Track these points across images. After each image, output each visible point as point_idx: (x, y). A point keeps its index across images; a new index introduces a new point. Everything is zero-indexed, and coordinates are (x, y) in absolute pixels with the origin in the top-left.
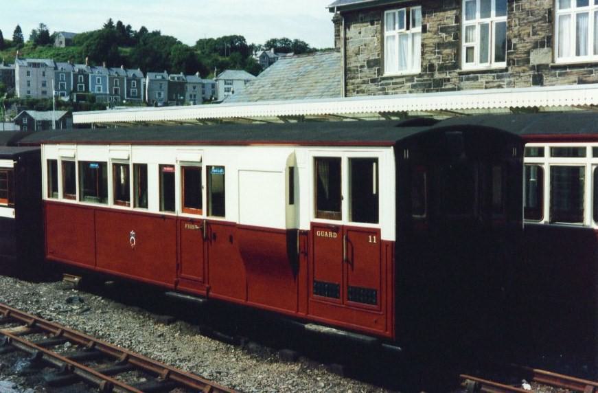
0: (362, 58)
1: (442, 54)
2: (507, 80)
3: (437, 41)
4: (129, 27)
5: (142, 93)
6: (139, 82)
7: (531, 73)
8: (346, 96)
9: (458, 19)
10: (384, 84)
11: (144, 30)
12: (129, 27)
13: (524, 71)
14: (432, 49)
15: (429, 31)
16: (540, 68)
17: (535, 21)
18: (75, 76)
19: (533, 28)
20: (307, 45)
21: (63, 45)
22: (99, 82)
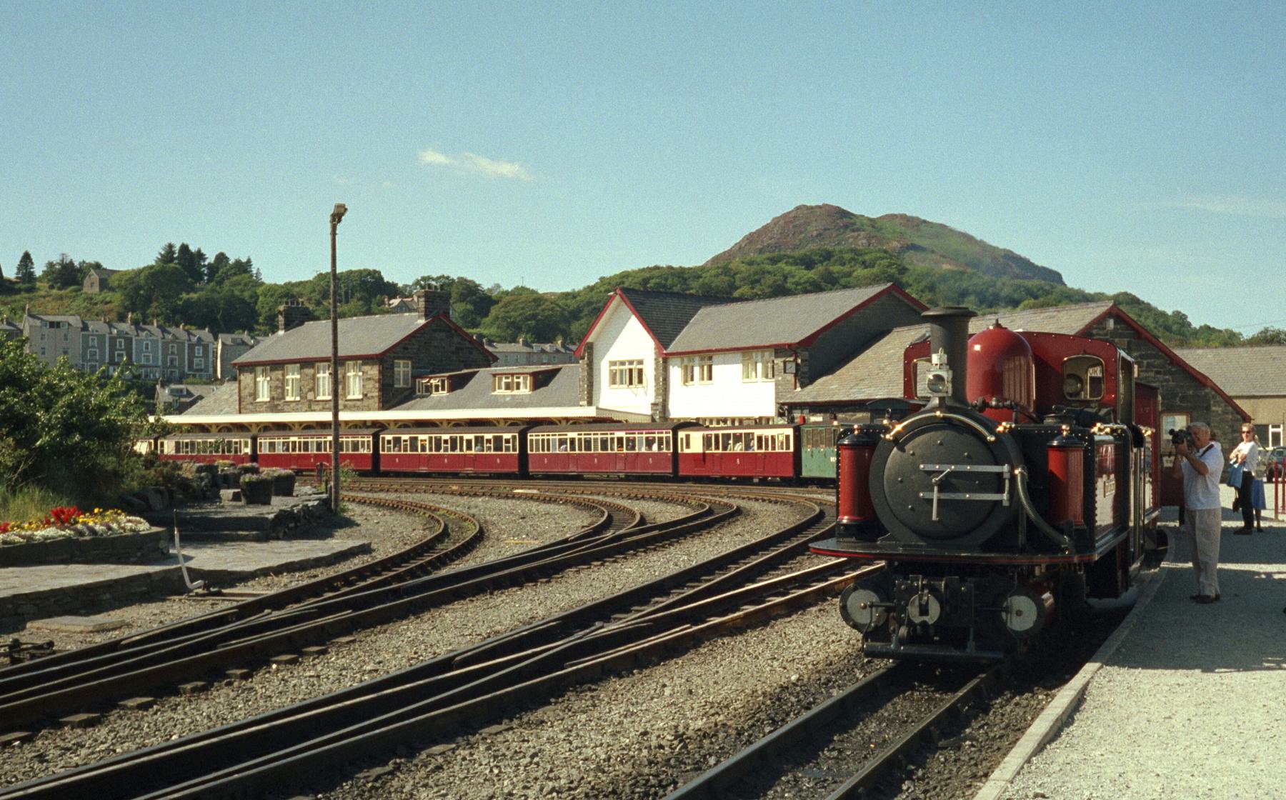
0: (247, 391)
5: (211, 366)
6: (206, 347)
8: (240, 412)
9: (283, 375)
10: (256, 408)
11: (221, 258)
16: (310, 401)
18: (113, 340)
20: (479, 285)
21: (96, 289)
22: (147, 348)
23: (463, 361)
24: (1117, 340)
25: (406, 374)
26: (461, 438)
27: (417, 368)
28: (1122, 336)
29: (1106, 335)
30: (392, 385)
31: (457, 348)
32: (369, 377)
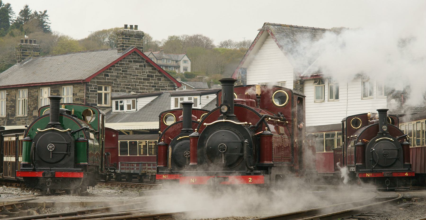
1: (11, 110)
2: (27, 121)
3: (10, 105)
7: (33, 119)
13: (31, 118)
14: (9, 108)
15: (8, 101)
17: (34, 100)
19: (34, 102)
23: (153, 86)
27: (116, 91)
31: (148, 76)
32: (78, 97)
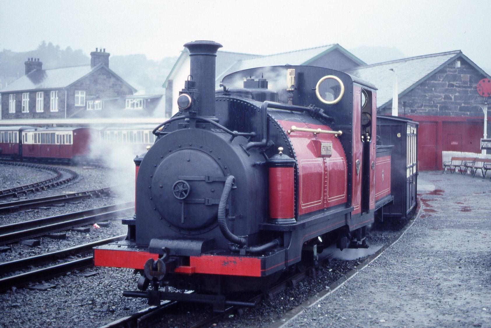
4: (58, 47)
11: (69, 48)
12: (58, 47)
24: (462, 75)
25: (82, 98)
26: (143, 132)
28: (465, 73)
29: (455, 71)
30: (74, 105)
